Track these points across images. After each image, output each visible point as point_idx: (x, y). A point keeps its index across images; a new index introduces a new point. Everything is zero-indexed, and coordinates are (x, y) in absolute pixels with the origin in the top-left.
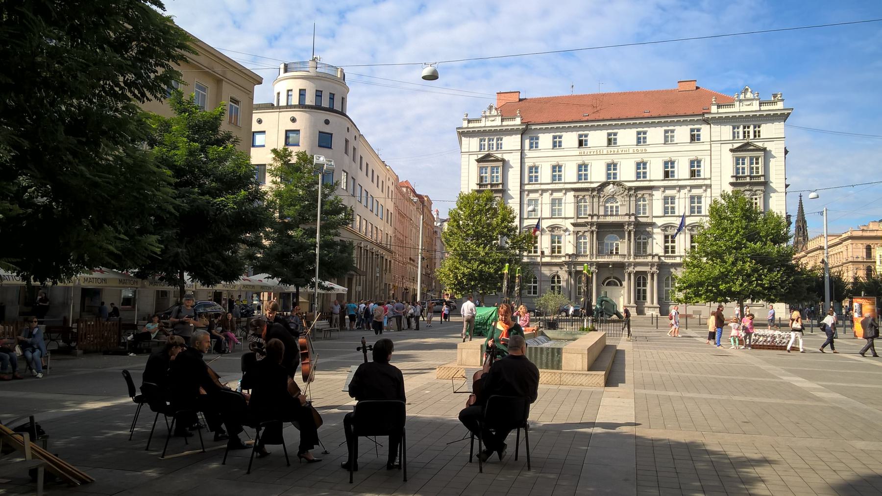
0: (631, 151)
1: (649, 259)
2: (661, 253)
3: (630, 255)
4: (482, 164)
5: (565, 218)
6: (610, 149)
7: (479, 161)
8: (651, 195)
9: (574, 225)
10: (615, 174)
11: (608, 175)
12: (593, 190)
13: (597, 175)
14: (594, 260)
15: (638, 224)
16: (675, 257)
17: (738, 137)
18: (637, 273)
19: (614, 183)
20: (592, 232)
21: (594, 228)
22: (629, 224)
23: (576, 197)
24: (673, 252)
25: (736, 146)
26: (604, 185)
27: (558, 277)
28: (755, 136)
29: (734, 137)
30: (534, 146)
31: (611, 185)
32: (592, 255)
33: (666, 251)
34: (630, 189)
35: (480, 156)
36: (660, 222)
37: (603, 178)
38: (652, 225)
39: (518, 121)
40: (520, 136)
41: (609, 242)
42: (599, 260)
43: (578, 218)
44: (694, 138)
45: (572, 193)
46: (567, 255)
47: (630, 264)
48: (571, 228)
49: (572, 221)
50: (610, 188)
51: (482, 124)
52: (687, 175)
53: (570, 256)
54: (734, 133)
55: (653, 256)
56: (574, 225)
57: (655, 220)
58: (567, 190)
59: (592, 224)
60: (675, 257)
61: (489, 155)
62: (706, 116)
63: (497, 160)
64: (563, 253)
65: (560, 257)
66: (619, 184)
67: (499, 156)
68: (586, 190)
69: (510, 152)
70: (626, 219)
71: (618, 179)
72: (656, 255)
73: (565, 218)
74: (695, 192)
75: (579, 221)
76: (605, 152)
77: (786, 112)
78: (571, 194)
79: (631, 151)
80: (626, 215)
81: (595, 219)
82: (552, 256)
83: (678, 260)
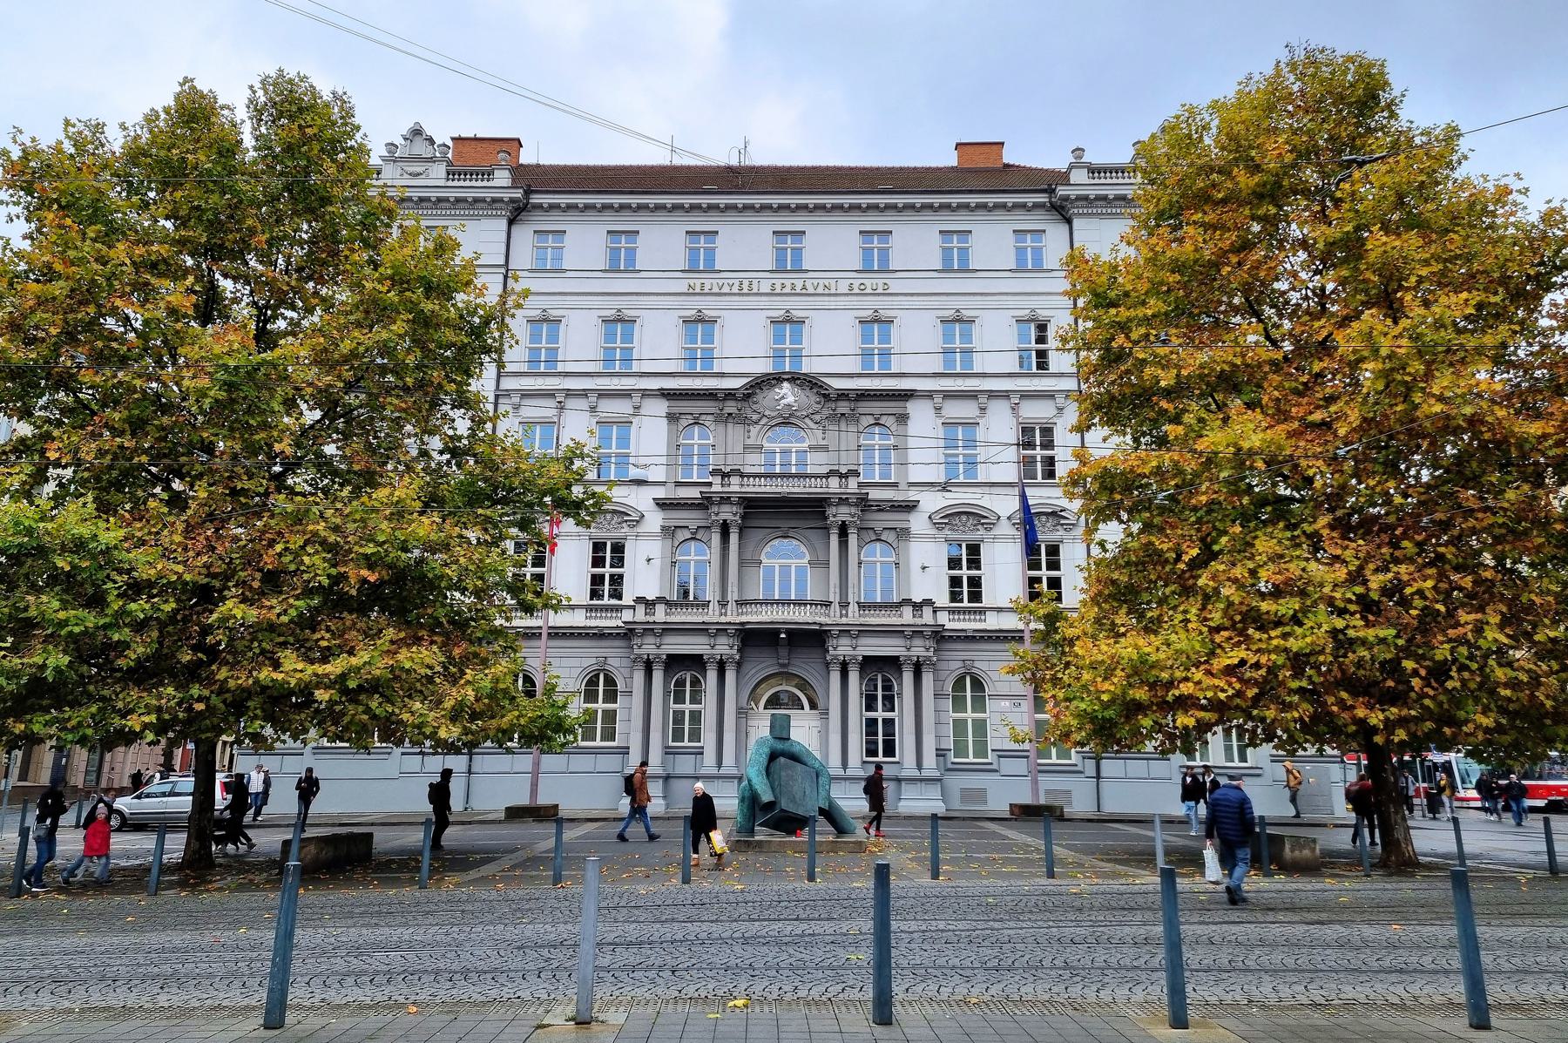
0: (843, 287)
1: (907, 615)
2: (943, 599)
3: (844, 605)
5: (640, 482)
6: (778, 281)
8: (903, 418)
9: (662, 504)
10: (797, 356)
11: (778, 356)
12: (730, 395)
16: (982, 611)
18: (869, 663)
19: (795, 379)
20: (725, 529)
21: (728, 513)
22: (843, 501)
23: (672, 418)
24: (976, 596)
26: (763, 383)
27: (610, 681)
31: (785, 384)
32: (723, 603)
33: (955, 596)
34: (843, 395)
36: (932, 502)
37: (763, 367)
38: (910, 507)
40: (504, 223)
41: (776, 563)
42: (744, 619)
43: (678, 484)
45: (662, 407)
46: (640, 600)
47: (844, 633)
48: (655, 520)
49: (661, 493)
50: (787, 394)
52: (1010, 363)
53: (650, 605)
55: (918, 607)
56: (662, 504)
57: (913, 495)
58: (646, 394)
59: (725, 500)
60: (982, 611)
62: (1062, 191)
64: (627, 599)
65: (619, 609)
66: (810, 383)
68: (710, 395)
70: (834, 484)
72: (928, 602)
73: (640, 482)
74: (1036, 412)
76: (766, 288)
79: (843, 287)
80: (832, 473)
81: (735, 486)
82: (589, 608)
83: (992, 622)
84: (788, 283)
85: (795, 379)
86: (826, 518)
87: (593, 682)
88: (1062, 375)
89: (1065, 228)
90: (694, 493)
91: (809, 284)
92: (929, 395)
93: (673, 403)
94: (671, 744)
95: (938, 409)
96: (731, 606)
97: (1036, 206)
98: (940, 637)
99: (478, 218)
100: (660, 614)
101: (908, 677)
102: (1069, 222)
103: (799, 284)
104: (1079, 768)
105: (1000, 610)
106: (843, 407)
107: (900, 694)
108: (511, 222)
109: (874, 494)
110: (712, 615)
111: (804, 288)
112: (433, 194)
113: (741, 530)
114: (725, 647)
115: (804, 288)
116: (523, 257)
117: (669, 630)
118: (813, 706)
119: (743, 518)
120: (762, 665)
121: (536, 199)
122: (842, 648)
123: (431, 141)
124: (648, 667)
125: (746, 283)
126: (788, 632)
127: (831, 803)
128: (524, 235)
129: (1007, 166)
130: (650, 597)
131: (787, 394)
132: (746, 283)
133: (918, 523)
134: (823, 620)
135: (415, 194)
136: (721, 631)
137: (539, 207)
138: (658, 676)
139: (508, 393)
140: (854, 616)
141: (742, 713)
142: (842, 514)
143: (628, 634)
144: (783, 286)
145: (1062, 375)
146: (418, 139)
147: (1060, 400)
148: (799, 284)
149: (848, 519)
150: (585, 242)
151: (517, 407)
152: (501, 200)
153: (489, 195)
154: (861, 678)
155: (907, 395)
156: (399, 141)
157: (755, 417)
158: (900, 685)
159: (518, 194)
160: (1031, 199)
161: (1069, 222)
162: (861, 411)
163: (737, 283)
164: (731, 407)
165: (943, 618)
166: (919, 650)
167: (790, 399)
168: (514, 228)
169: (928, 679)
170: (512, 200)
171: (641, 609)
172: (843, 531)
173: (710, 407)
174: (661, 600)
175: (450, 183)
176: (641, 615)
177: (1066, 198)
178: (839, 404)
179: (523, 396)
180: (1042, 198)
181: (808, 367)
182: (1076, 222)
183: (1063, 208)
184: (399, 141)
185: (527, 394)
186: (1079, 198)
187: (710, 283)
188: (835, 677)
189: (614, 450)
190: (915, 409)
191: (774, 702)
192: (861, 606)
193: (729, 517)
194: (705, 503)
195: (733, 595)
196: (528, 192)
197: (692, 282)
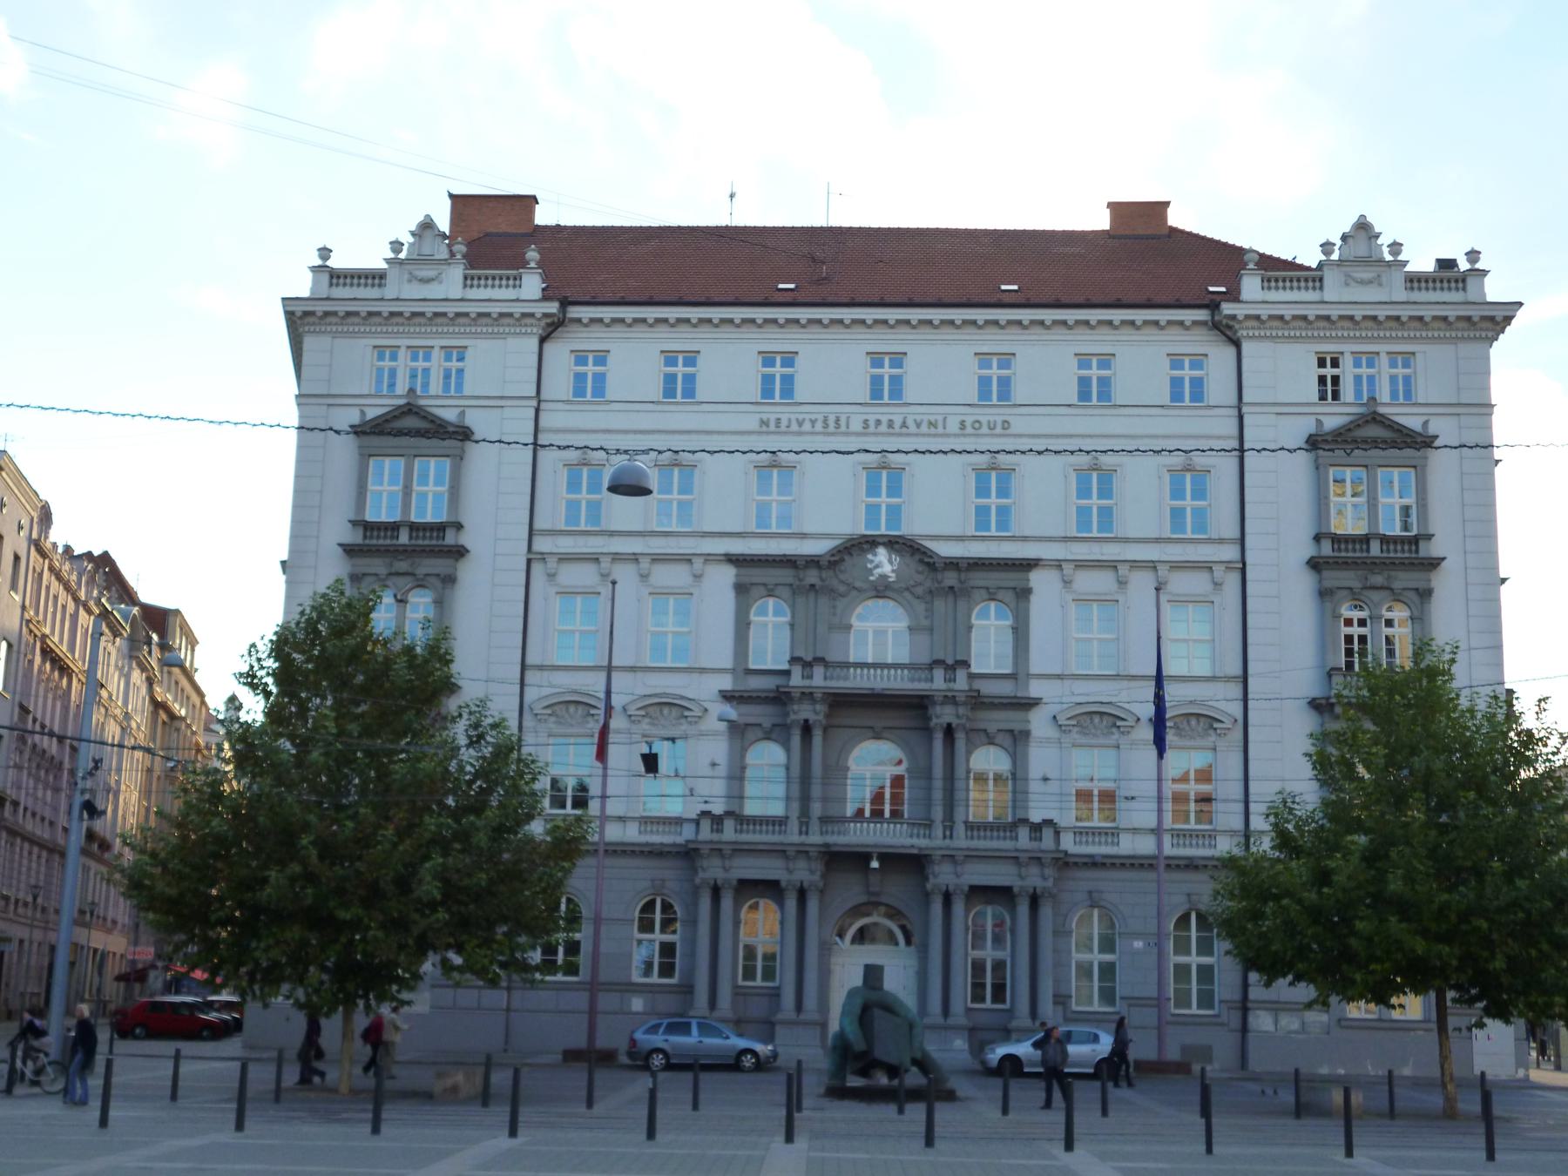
4: (376, 441)
5: (702, 670)
6: (873, 414)
7: (358, 431)
8: (1024, 593)
10: (894, 512)
12: (813, 562)
13: (827, 507)
14: (815, 838)
15: (977, 702)
17: (1336, 396)
20: (807, 729)
22: (951, 700)
23: (741, 589)
25: (1331, 423)
28: (1394, 394)
29: (1323, 397)
30: (591, 388)
34: (953, 564)
35: (372, 413)
38: (1030, 704)
39: (532, 285)
40: (533, 343)
42: (831, 839)
44: (1186, 392)
45: (728, 574)
46: (705, 814)
49: (726, 683)
51: (390, 291)
53: (717, 821)
54: (1322, 380)
55: (1036, 829)
57: (1035, 689)
58: (709, 558)
59: (808, 696)
61: (410, 410)
67: (449, 415)
69: (499, 401)
70: (939, 681)
71: (905, 530)
72: (1049, 822)
75: (755, 683)
77: (1499, 314)
78: (726, 576)
81: (819, 679)
83: (1128, 845)
84: (884, 419)
85: (897, 544)
86: (930, 719)
87: (649, 907)
88: (1221, 541)
89: (1232, 351)
90: (768, 683)
91: (910, 422)
92: (1058, 565)
93: (744, 571)
94: (740, 982)
95: (1067, 583)
96: (815, 826)
97: (1195, 323)
98: (1065, 863)
99: (502, 336)
100: (729, 832)
101: (1023, 909)
102: (1237, 344)
103: (898, 421)
104: (1224, 1019)
105: (1135, 831)
106: (950, 579)
107: (1013, 931)
108: (543, 340)
109: (988, 688)
110: (793, 836)
111: (904, 425)
112: (451, 309)
113: (825, 730)
114: (805, 873)
115: (904, 425)
116: (559, 382)
117: (740, 850)
118: (908, 942)
119: (828, 716)
120: (849, 891)
121: (574, 312)
122: (943, 876)
124: (716, 891)
125: (832, 419)
126: (883, 857)
127: (925, 1054)
128: (560, 353)
129: (1174, 230)
130: (718, 808)
131: (884, 563)
132: (832, 419)
133: (1038, 723)
134: (922, 842)
135: (429, 309)
136: (803, 852)
137: (579, 321)
138: (727, 903)
139: (543, 557)
140: (961, 841)
141: (826, 950)
142: (944, 715)
143: (688, 854)
144: (878, 422)
145: (1221, 541)
146: (428, 233)
147: (1219, 571)
148: (898, 421)
149: (955, 722)
150: (633, 353)
151: (552, 576)
152: (532, 315)
153: (517, 309)
154: (967, 911)
155: (1029, 565)
157: (842, 589)
158: (1013, 919)
159: (553, 307)
160: (1189, 315)
161: (1237, 344)
162: (972, 583)
163: (820, 418)
164: (812, 577)
165: (1068, 843)
166: (1034, 879)
167: (887, 569)
168: (547, 346)
169: (1046, 912)
170: (546, 315)
171: (706, 825)
172: (949, 731)
173: (785, 575)
174: (729, 814)
175: (474, 293)
176: (706, 833)
177: (1234, 317)
178: (946, 581)
179: (560, 560)
180: (1202, 315)
181: (912, 526)
182: (1246, 347)
183: (1230, 327)
184: (407, 239)
185: (565, 558)
186: (1248, 317)
187: (786, 414)
188: (937, 908)
189: (671, 628)
190: (1036, 578)
191: (862, 937)
192: (970, 826)
193: (812, 717)
194: (780, 699)
195: (816, 809)
196: (565, 303)
197: (765, 417)
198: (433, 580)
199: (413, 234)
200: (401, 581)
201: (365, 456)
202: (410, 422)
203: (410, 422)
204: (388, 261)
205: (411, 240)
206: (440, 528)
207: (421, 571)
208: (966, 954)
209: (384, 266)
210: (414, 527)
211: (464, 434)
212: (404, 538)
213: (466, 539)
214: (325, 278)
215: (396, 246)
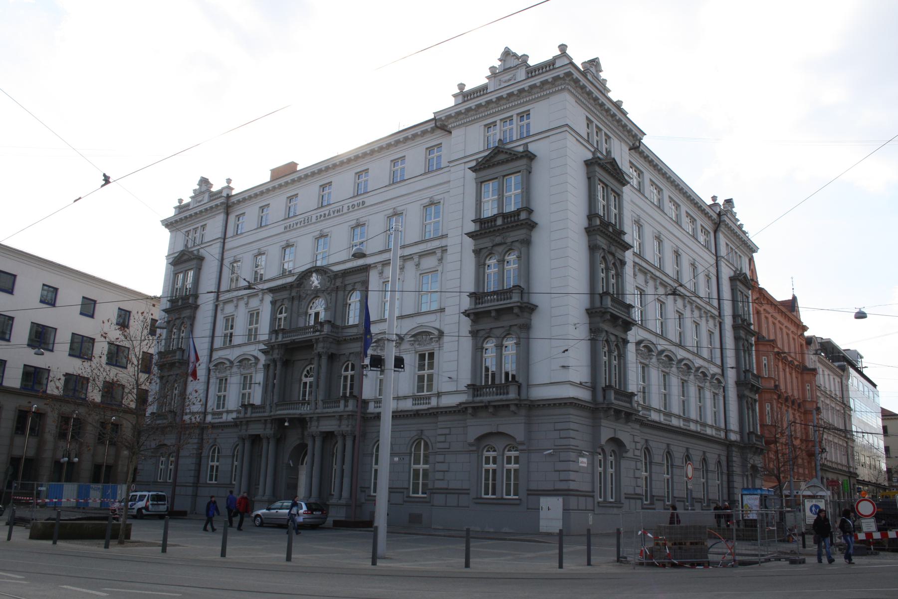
61: (497, 151)
63: (514, 157)
67: (521, 149)
99: (547, 96)
123: (515, 55)
146: (509, 57)
156: (497, 64)
198: (517, 244)
199: (500, 60)
200: (500, 249)
201: (480, 183)
202: (502, 157)
203: (502, 157)
204: (488, 78)
205: (500, 63)
206: (517, 213)
207: (509, 240)
208: (503, 467)
209: (487, 81)
210: (504, 216)
211: (530, 157)
212: (499, 222)
213: (535, 218)
214: (461, 97)
215: (492, 69)
